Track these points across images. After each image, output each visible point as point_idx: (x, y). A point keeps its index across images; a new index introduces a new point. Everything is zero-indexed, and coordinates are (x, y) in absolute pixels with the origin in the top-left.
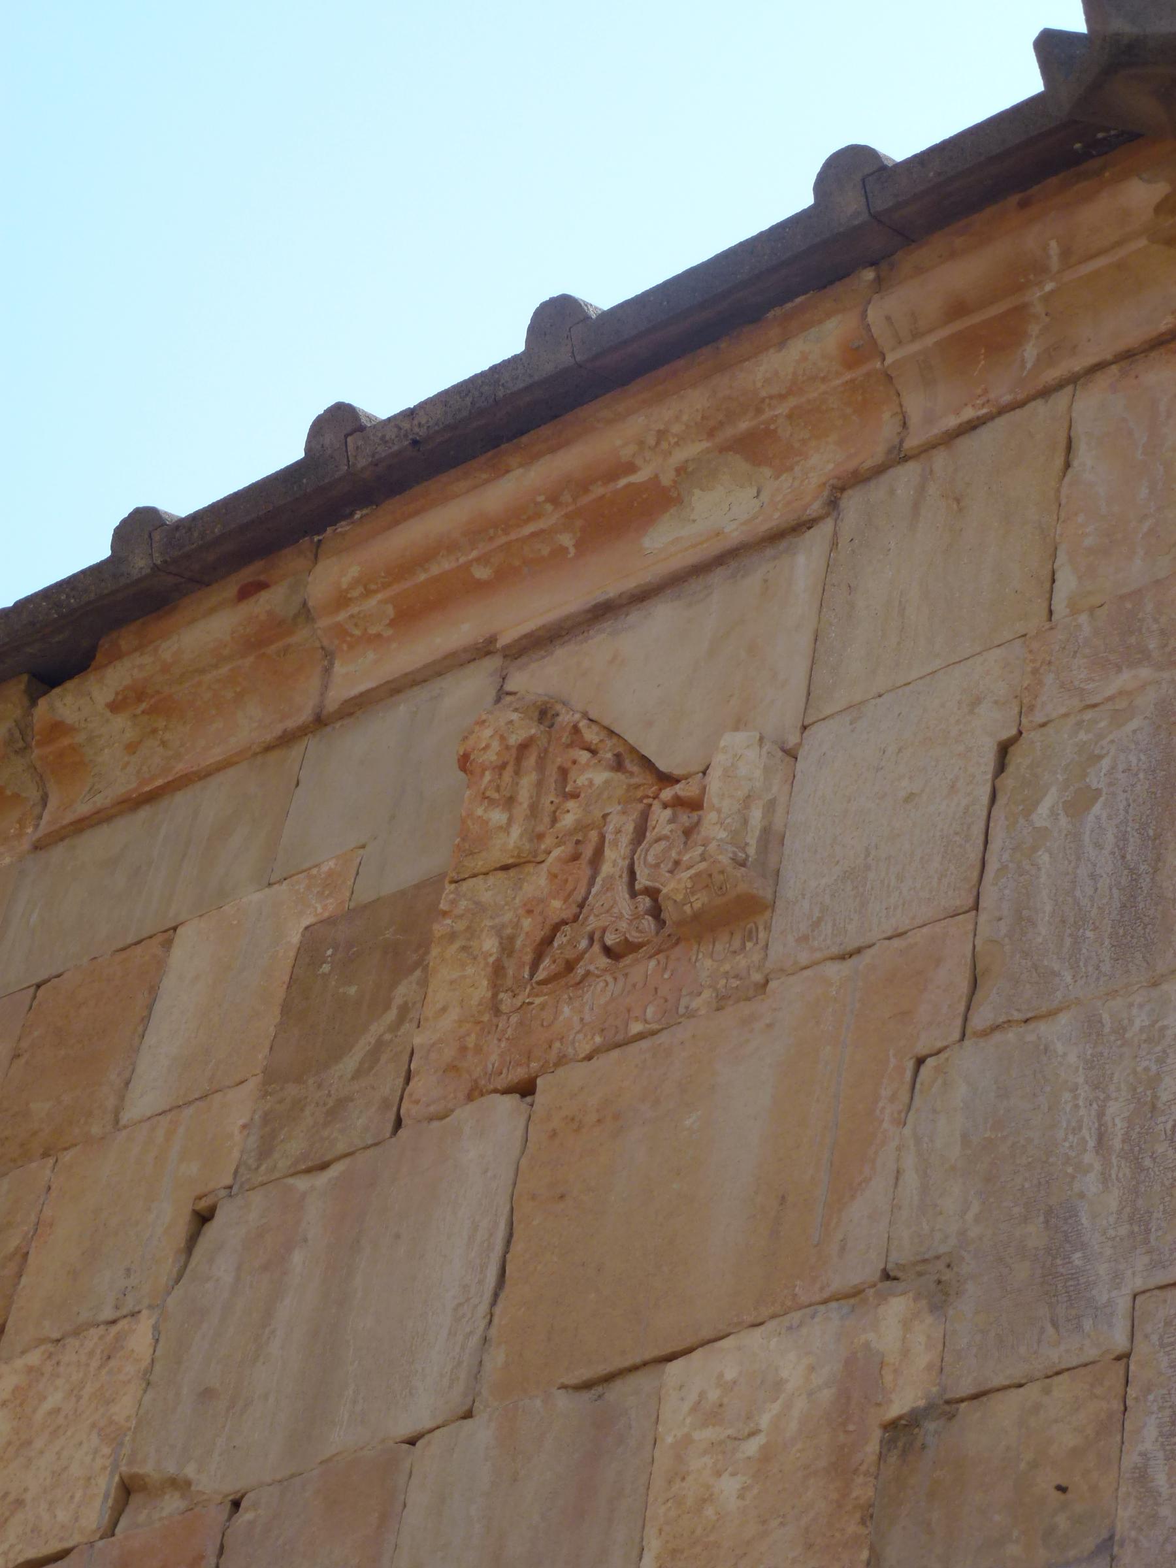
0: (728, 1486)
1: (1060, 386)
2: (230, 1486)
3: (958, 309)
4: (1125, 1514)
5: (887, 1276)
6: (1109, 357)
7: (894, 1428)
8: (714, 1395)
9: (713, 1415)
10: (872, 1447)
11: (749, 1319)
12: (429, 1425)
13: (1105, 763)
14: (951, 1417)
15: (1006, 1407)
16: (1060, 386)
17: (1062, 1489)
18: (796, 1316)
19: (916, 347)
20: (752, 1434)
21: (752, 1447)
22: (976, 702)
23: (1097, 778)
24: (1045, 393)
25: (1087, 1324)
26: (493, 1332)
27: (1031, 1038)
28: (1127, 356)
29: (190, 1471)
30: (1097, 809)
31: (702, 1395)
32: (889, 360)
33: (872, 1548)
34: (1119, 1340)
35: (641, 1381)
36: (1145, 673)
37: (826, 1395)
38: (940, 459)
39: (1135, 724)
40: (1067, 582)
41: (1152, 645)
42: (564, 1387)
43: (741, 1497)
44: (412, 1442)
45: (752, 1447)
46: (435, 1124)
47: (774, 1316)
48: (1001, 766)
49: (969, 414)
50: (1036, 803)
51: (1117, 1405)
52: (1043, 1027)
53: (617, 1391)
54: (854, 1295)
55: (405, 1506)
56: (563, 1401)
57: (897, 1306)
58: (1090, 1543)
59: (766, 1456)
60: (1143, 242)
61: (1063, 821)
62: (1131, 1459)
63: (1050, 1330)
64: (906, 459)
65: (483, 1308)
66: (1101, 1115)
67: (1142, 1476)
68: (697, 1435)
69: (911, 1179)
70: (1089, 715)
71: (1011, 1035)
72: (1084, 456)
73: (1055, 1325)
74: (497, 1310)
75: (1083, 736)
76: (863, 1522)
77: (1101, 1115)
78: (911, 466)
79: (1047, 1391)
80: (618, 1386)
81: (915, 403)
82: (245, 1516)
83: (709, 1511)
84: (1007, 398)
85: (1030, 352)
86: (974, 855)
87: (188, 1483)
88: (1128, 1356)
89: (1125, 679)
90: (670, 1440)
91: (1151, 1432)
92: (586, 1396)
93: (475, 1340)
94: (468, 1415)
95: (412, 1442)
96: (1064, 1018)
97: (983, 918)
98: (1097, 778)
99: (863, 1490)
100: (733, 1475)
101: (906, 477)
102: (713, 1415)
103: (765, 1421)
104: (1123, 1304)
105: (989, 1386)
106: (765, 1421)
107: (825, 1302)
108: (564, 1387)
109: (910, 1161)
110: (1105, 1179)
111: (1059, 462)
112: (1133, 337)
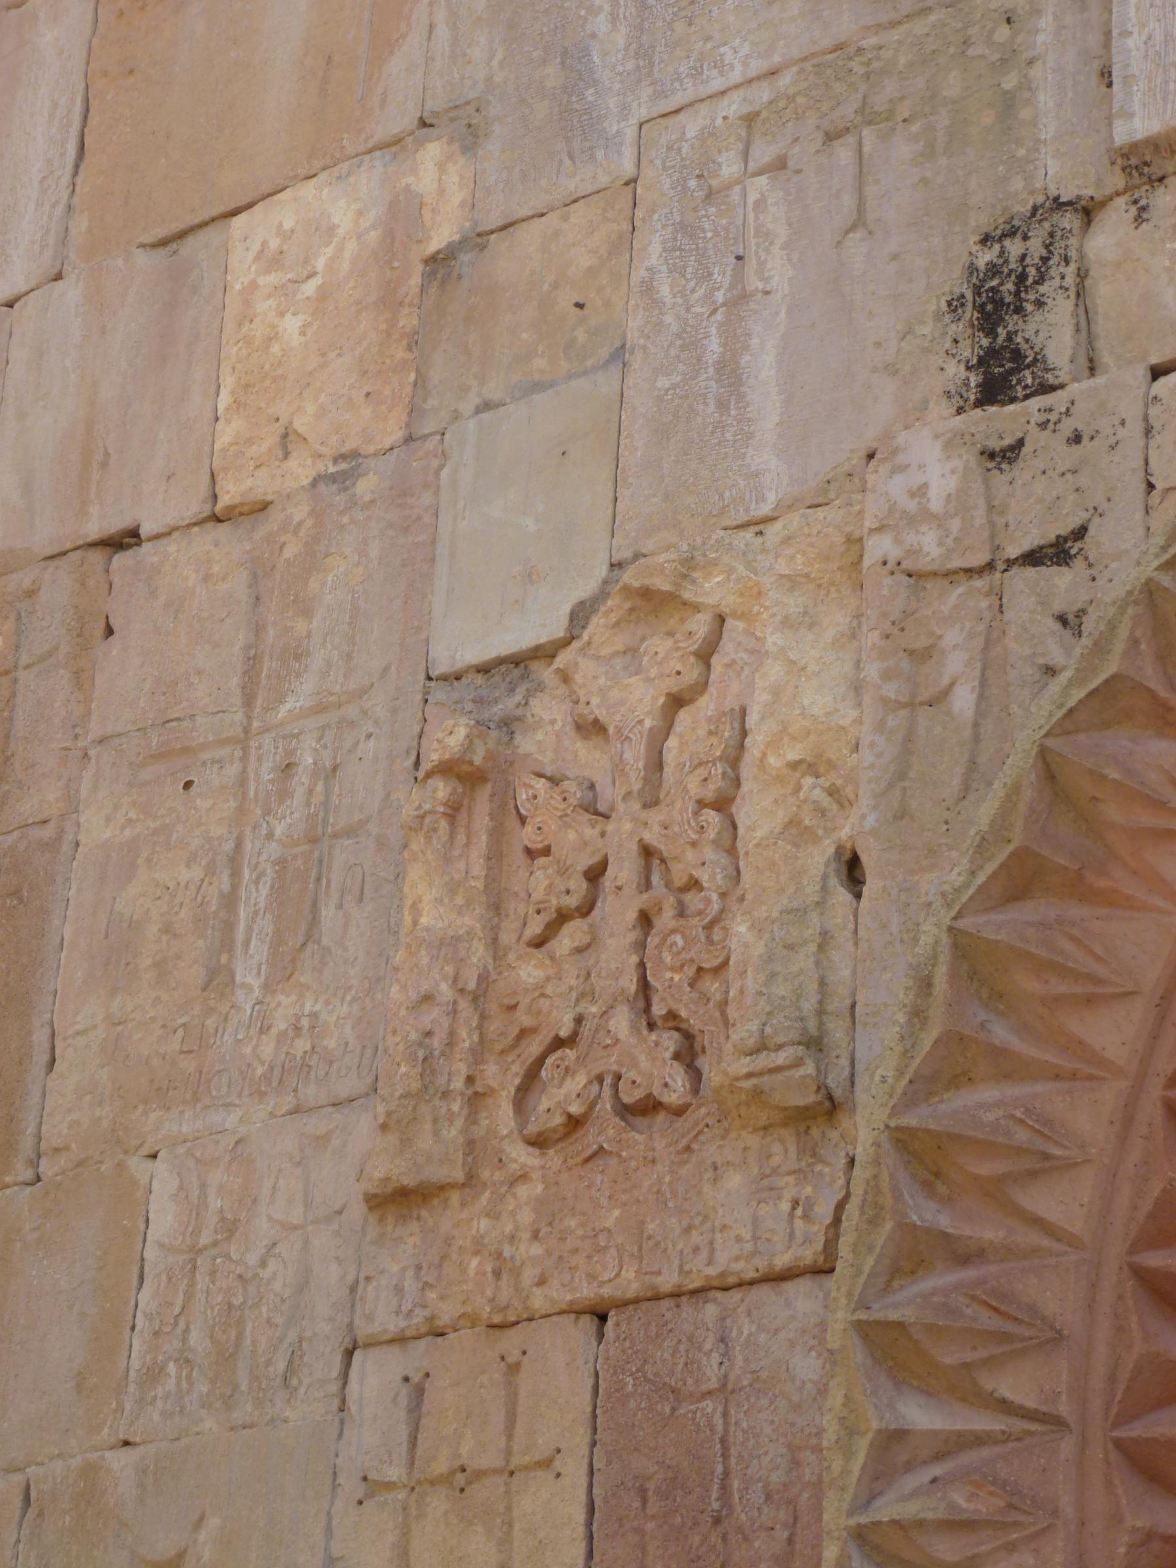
0: (291, 325)
4: (634, 324)
5: (423, 124)
7: (435, 262)
8: (274, 244)
9: (275, 262)
10: (415, 280)
11: (302, 172)
12: (24, 289)
14: (483, 248)
15: (530, 236)
17: (580, 306)
18: (344, 167)
20: (311, 276)
21: (310, 288)
25: (600, 154)
26: (76, 200)
31: (264, 244)
33: (418, 370)
34: (628, 167)
35: (211, 236)
37: (373, 236)
42: (142, 246)
43: (302, 333)
44: (10, 305)
45: (310, 288)
46: (13, 12)
47: (324, 169)
51: (626, 226)
53: (191, 244)
54: (395, 143)
55: (8, 362)
56: (142, 259)
57: (433, 150)
58: (605, 352)
59: (323, 294)
62: (639, 274)
63: (567, 161)
65: (66, 179)
67: (648, 288)
68: (262, 281)
69: (442, 32)
73: (571, 157)
74: (79, 180)
76: (409, 348)
79: (565, 218)
80: (190, 241)
83: (275, 349)
88: (635, 180)
90: (238, 287)
91: (655, 249)
92: (163, 252)
93: (60, 210)
94: (58, 277)
95: (10, 305)
99: (408, 320)
100: (294, 314)
102: (275, 262)
103: (320, 264)
104: (630, 133)
105: (515, 218)
106: (320, 264)
107: (370, 151)
108: (142, 246)
109: (441, 15)
110: (614, 18)
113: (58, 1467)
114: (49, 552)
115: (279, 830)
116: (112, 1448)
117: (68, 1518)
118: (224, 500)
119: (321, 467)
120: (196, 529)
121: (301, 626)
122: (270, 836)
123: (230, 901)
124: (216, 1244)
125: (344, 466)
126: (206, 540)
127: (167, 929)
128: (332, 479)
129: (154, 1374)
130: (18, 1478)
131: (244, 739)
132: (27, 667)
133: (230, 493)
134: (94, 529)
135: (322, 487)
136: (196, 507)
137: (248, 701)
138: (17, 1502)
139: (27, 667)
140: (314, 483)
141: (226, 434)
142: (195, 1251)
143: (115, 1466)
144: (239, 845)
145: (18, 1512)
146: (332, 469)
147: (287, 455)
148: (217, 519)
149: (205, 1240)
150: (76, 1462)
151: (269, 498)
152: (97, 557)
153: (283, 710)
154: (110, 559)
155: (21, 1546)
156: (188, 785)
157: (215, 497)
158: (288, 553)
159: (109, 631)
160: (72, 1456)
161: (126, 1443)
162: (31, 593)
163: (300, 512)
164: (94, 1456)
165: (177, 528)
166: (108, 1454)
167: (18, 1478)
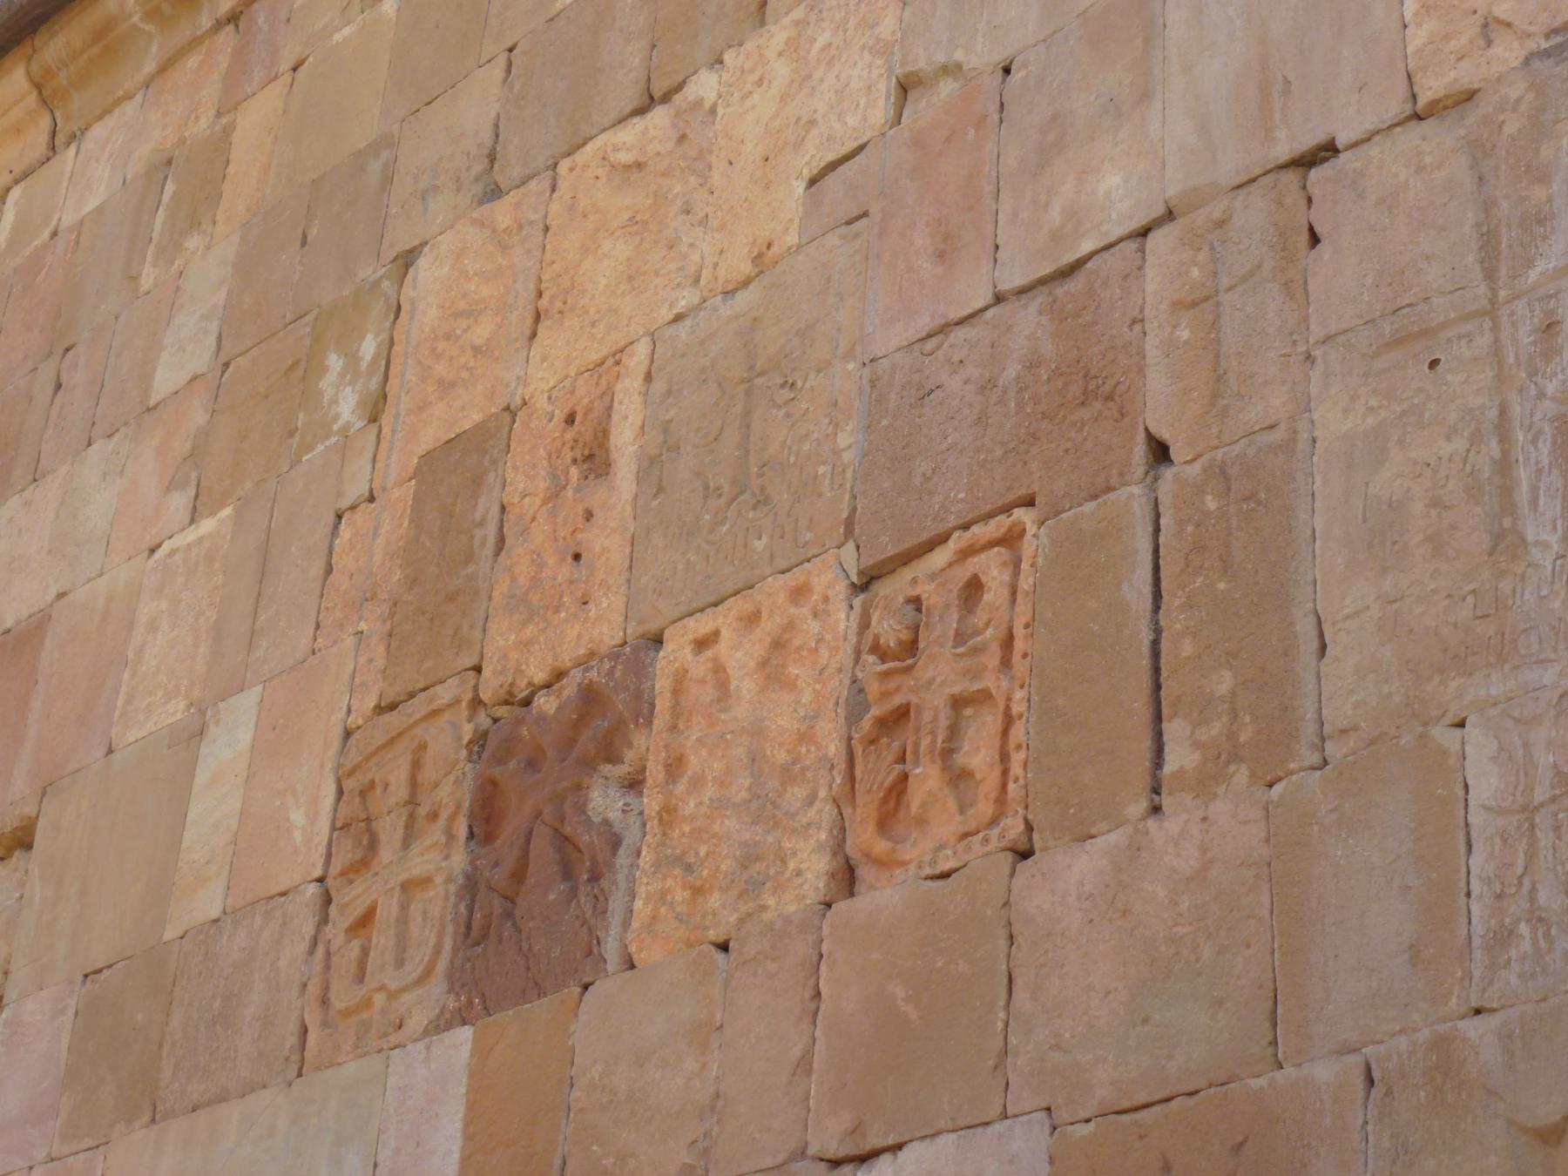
2: (999, 57)
29: (959, 55)
55: (1165, 26)
82: (1017, 76)
87: (959, 66)
113: (1402, 1043)
114: (1237, 181)
115: (1551, 388)
116: (1463, 1018)
117: (1422, 1093)
118: (1422, 101)
119: (1531, 45)
120: (1398, 129)
121: (1539, 193)
122: (1541, 395)
123: (1504, 466)
124: (1554, 799)
125: (1559, 39)
126: (1412, 136)
127: (1436, 503)
128: (1547, 53)
129: (1502, 938)
130: (1354, 1060)
131: (1492, 310)
132: (1229, 289)
133: (1431, 88)
134: (1284, 150)
135: (1536, 64)
136: (1396, 107)
137: (1490, 275)
138: (1359, 1082)
139: (1229, 289)
140: (1527, 61)
141: (1417, 38)
142: (1530, 810)
143: (1472, 1034)
144: (1503, 411)
145: (1361, 1094)
146: (1544, 45)
147: (1489, 43)
148: (1418, 117)
149: (1540, 795)
150: (1424, 1035)
151: (1476, 86)
152: (1290, 178)
153: (1533, 275)
154: (1305, 178)
155: (1370, 1128)
156: (1434, 364)
157: (1414, 97)
158: (1509, 129)
159: (1314, 239)
160: (1415, 1030)
161: (1478, 1012)
162: (1221, 224)
163: (1516, 90)
164: (1443, 1028)
165: (1377, 132)
166: (1461, 1024)
167: (1354, 1060)
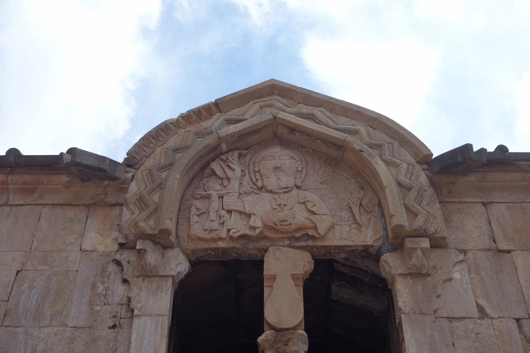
1: (40, 205)
3: (25, 183)
6: (50, 203)
13: (37, 282)
16: (40, 205)
19: (15, 186)
22: (14, 260)
23: (35, 284)
24: (37, 205)
27: (15, 330)
28: (53, 205)
30: (34, 290)
32: (9, 187)
36: (47, 268)
38: (14, 208)
39: (44, 277)
40: (35, 244)
41: (49, 263)
48: (17, 275)
49: (21, 202)
50: (23, 285)
52: (17, 329)
60: (61, 186)
61: (28, 290)
64: (8, 205)
66: (25, 349)
70: (35, 272)
71: (11, 328)
72: (43, 220)
75: (34, 275)
77: (25, 349)
78: (8, 207)
81: (11, 196)
84: (29, 203)
85: (35, 196)
86: (9, 291)
89: (43, 267)
96: (21, 329)
97: (9, 304)
98: (35, 284)
101: (7, 209)
111: (37, 220)
112: (55, 202)
